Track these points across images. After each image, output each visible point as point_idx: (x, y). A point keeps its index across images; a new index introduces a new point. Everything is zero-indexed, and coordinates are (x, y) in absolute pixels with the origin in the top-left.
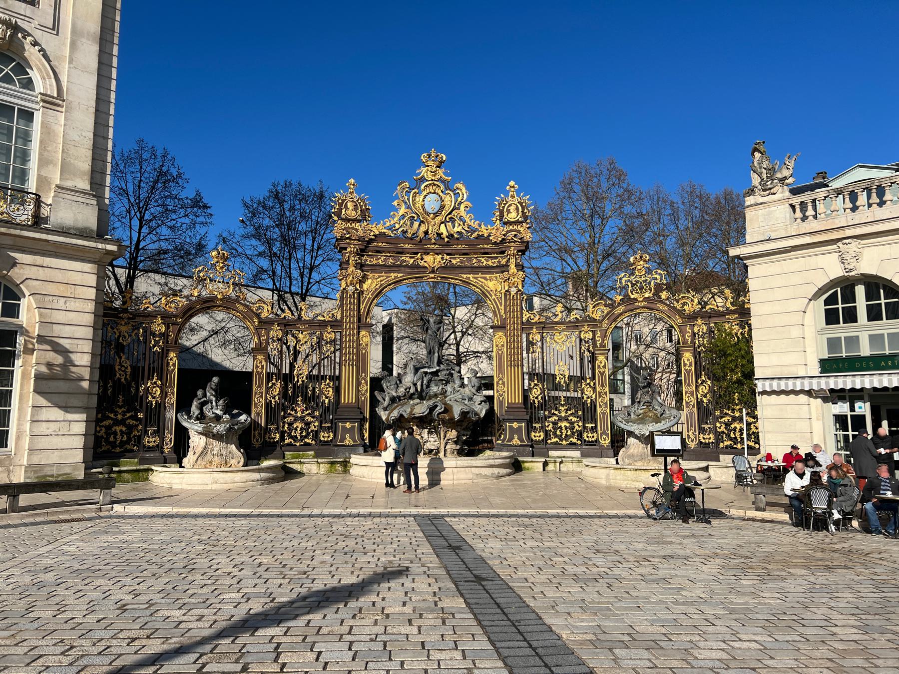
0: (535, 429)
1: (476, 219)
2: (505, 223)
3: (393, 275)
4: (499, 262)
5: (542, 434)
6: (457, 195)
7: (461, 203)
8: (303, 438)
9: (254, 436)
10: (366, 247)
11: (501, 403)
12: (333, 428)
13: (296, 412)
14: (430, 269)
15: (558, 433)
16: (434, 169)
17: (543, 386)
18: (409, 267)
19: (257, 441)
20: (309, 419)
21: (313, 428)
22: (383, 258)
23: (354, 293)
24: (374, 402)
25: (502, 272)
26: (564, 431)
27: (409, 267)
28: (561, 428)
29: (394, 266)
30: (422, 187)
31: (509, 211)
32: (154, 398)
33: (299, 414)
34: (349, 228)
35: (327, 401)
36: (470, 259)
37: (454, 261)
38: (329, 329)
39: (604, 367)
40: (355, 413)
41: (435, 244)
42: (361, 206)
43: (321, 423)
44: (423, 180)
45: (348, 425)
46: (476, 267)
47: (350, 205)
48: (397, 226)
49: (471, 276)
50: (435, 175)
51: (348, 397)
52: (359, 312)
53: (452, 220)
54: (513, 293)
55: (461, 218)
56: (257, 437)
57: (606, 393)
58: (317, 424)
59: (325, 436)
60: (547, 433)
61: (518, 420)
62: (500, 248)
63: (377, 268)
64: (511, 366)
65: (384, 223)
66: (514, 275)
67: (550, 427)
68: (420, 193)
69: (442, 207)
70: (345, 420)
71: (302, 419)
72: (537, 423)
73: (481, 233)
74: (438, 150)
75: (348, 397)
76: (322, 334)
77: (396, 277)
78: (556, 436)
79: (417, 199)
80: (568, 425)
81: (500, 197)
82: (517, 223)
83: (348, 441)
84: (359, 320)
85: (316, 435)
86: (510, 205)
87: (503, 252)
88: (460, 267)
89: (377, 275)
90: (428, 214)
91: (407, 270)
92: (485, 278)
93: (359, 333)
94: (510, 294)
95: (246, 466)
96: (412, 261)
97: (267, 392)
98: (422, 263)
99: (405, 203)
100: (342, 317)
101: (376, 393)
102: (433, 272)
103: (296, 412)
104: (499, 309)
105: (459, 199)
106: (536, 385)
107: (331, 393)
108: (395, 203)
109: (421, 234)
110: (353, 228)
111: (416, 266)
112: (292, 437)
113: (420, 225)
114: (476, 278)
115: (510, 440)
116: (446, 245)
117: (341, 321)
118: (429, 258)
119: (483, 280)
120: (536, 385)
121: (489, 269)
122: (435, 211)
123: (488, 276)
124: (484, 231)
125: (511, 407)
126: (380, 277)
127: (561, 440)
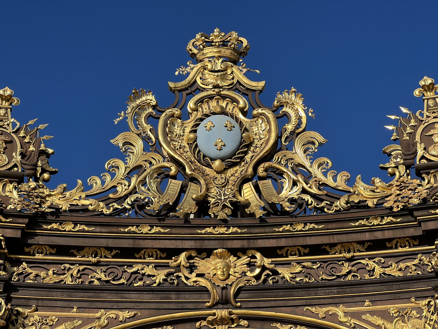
1: (337, 168)
2: (420, 173)
6: (283, 118)
7: (294, 134)
10: (26, 234)
14: (216, 294)
16: (219, 65)
18: (153, 291)
22: (75, 270)
27: (153, 291)
30: (191, 104)
37: (286, 273)
41: (225, 223)
44: (193, 88)
48: (121, 190)
49: (340, 311)
50: (223, 78)
53: (276, 175)
55: (298, 168)
65: (87, 187)
68: (184, 116)
69: (245, 145)
74: (226, 29)
79: (177, 130)
90: (206, 160)
91: (147, 297)
92: (385, 315)
96: (160, 275)
102: (224, 302)
105: (290, 127)
111: (174, 288)
116: (259, 230)
118: (212, 266)
122: (227, 151)
123: (392, 308)
124: (363, 191)
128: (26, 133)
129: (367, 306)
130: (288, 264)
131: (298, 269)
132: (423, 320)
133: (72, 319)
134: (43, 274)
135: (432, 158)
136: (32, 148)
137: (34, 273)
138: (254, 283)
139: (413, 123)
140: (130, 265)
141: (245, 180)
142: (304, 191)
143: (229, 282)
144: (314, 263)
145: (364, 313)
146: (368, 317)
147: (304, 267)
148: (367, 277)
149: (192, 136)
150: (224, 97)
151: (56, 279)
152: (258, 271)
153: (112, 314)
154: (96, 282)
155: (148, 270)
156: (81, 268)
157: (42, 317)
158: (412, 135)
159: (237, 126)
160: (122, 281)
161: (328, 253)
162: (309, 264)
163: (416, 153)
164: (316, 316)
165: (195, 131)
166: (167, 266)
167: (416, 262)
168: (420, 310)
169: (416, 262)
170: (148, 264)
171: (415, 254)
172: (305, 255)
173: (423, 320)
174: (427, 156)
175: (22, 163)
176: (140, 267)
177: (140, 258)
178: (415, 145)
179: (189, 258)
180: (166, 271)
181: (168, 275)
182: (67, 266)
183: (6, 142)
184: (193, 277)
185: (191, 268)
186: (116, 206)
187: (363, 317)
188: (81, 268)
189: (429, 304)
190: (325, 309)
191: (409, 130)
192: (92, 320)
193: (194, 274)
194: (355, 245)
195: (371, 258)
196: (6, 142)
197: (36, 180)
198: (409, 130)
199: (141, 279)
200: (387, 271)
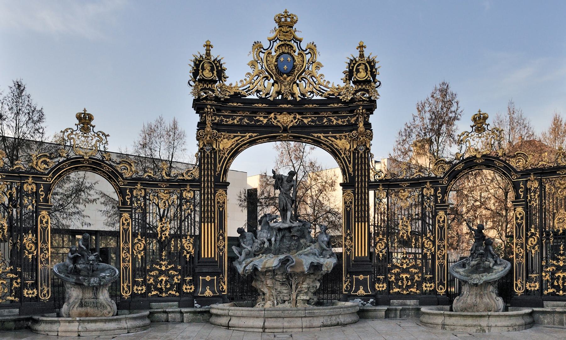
0: (379, 281)
3: (248, 135)
4: (348, 121)
5: (385, 285)
8: (167, 290)
9: (124, 289)
11: (348, 257)
12: (194, 282)
13: (161, 265)
15: (400, 284)
17: (387, 240)
19: (126, 293)
20: (173, 272)
21: (176, 281)
25: (351, 131)
26: (405, 282)
28: (402, 279)
29: (248, 125)
31: (358, 71)
32: (29, 253)
33: (163, 268)
34: (205, 89)
35: (188, 256)
36: (321, 119)
37: (306, 121)
39: (444, 221)
40: (213, 266)
42: (217, 67)
43: (183, 277)
45: (208, 278)
46: (326, 127)
49: (321, 135)
51: (208, 252)
52: (215, 171)
54: (361, 152)
56: (126, 289)
57: (444, 246)
58: (180, 277)
59: (187, 288)
60: (389, 284)
61: (364, 273)
63: (232, 129)
64: (358, 222)
67: (393, 279)
69: (294, 67)
70: (205, 274)
71: (165, 273)
72: (381, 275)
73: (331, 93)
75: (208, 252)
76: (181, 194)
77: (251, 137)
78: (399, 287)
80: (408, 276)
82: (367, 82)
83: (208, 293)
84: (217, 178)
85: (179, 287)
86: (360, 65)
87: (352, 111)
88: (310, 126)
89: (232, 135)
92: (335, 137)
93: (215, 193)
94: (358, 152)
95: (117, 315)
97: (133, 246)
98: (275, 122)
103: (161, 267)
104: (347, 167)
106: (380, 239)
110: (210, 89)
112: (156, 289)
113: (273, 85)
114: (326, 137)
115: (356, 291)
117: (199, 181)
119: (333, 139)
120: (380, 239)
121: (338, 129)
125: (357, 260)
126: (235, 137)
127: (403, 290)
129: (330, 134)
130: (306, 118)
131: (310, 120)
133: (238, 136)
134: (228, 120)
136: (220, 68)
140: (255, 117)
141: (294, 83)
144: (315, 117)
145: (329, 136)
146: (330, 138)
149: (276, 63)
150: (288, 45)
153: (250, 134)
155: (261, 119)
158: (353, 67)
164: (314, 137)
166: (267, 117)
168: (346, 136)
170: (261, 116)
179: (275, 114)
185: (275, 118)
189: (349, 135)
191: (352, 65)
195: (333, 117)
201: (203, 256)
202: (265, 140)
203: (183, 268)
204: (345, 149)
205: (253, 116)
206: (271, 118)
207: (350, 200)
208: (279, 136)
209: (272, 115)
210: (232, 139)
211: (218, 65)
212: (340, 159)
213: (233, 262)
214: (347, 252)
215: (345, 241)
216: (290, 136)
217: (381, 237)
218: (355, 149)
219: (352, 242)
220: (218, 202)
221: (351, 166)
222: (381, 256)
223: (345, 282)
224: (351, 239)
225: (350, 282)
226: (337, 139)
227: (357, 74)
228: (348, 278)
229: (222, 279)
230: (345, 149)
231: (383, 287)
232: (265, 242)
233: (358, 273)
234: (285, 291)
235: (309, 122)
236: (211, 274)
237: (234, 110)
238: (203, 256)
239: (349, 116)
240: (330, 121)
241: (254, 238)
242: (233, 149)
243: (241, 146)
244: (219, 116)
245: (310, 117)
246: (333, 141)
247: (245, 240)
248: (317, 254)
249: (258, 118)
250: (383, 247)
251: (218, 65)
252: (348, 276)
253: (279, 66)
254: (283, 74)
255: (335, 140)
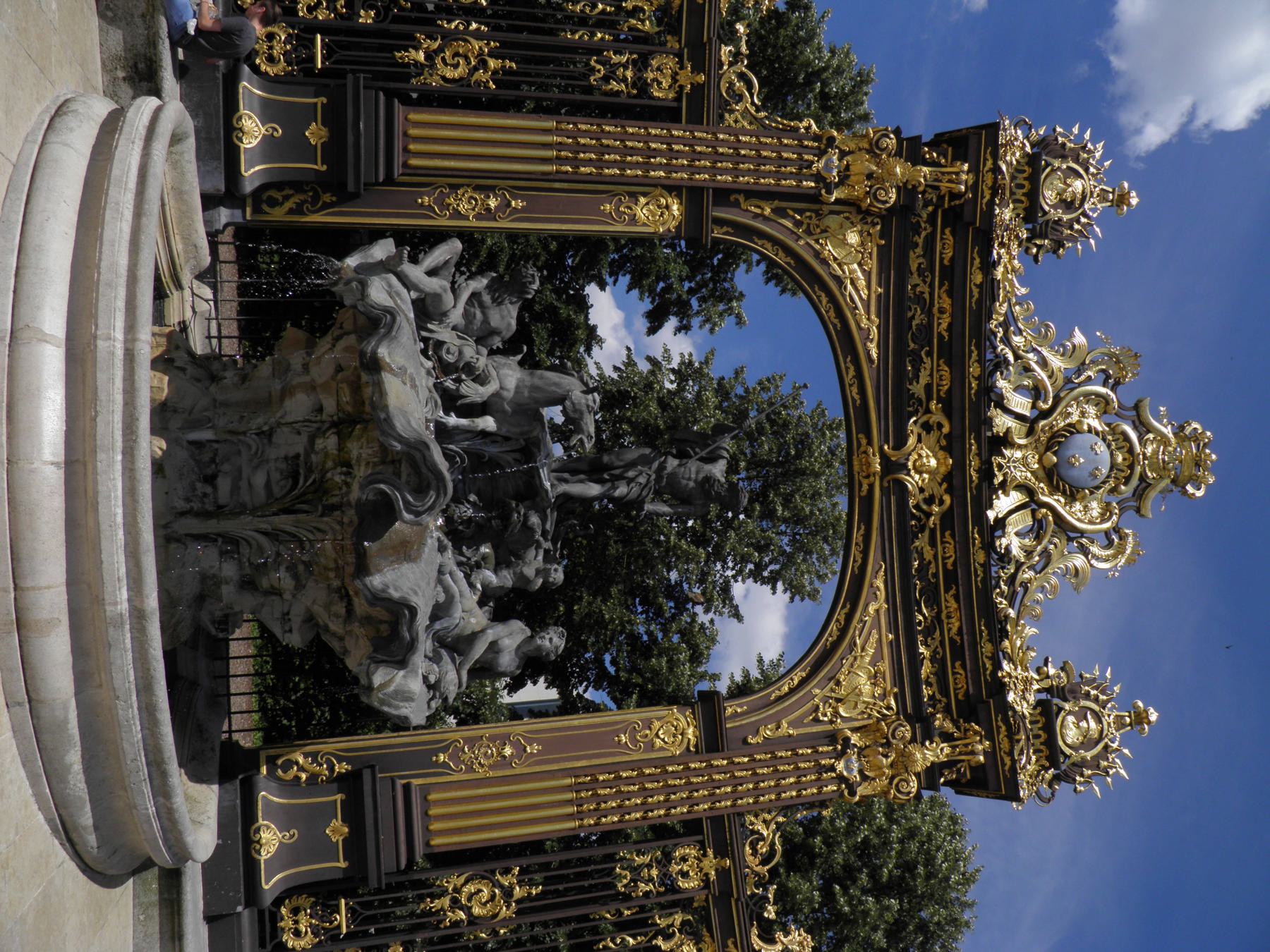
23: (818, 177)
24: (417, 242)
31: (1081, 715)
37: (922, 542)
38: (687, 78)
43: (324, 29)
47: (1078, 185)
48: (1017, 340)
54: (840, 766)
61: (355, 845)
62: (983, 703)
64: (577, 788)
66: (902, 764)
70: (334, 119)
75: (430, 135)
79: (1091, 410)
81: (1114, 681)
83: (253, 130)
84: (724, 195)
86: (1099, 719)
89: (872, 264)
96: (918, 389)
99: (1079, 372)
100: (729, 130)
101: (456, 245)
105: (1095, 549)
106: (508, 893)
107: (450, 73)
108: (1079, 338)
109: (1002, 422)
123: (885, 666)
126: (868, 275)
128: (1084, 225)
130: (933, 543)
131: (928, 555)
132: (871, 700)
134: (919, 251)
135: (1060, 719)
137: (920, 241)
138: (911, 502)
139: (1102, 697)
140: (929, 354)
142: (1019, 565)
143: (912, 472)
147: (930, 562)
148: (920, 638)
149: (1086, 427)
151: (914, 267)
152: (925, 507)
154: (910, 314)
156: (927, 296)
157: (870, 254)
158: (1087, 696)
159: (1097, 483)
160: (912, 345)
161: (946, 591)
162: (932, 570)
163: (1065, 700)
165: (1090, 431)
167: (938, 696)
168: (884, 696)
169: (938, 696)
170: (931, 375)
171: (947, 695)
172: (944, 565)
173: (871, 700)
174: (1063, 713)
175: (1048, 222)
176: (928, 366)
177: (938, 365)
178: (1076, 699)
180: (923, 397)
181: (920, 400)
182: (928, 280)
183: (1072, 202)
184: (916, 430)
186: (999, 335)
187: (874, 631)
188: (927, 296)
189: (889, 708)
190: (882, 586)
191: (1093, 692)
192: (868, 312)
193: (920, 430)
194: (957, 624)
195: (942, 643)
196: (1072, 202)
197: (1029, 240)
198: (1093, 692)
199: (913, 367)
200: (927, 663)
201: (413, 116)
202: (855, 390)
203: (365, 31)
204: (839, 700)
205: (930, 344)
206: (928, 411)
207: (658, 742)
208: (870, 443)
209: (937, 417)
210: (860, 265)
211: (1076, 226)
212: (803, 682)
213: (390, 241)
214: (444, 750)
215: (492, 739)
216: (871, 486)
217: (518, 892)
218: (847, 740)
219: (491, 767)
220: (634, 196)
221: (786, 729)
222: (437, 904)
223: (314, 756)
224: (504, 762)
225: (313, 778)
226: (873, 663)
227: (1070, 713)
228: (331, 768)
229: (314, 203)
230: (839, 700)
231: (297, 933)
232: (482, 385)
233: (353, 814)
234: (259, 480)
235: (921, 555)
236: (335, 149)
237: (953, 276)
238: (412, 116)
239: (948, 705)
240: (928, 632)
241: (497, 343)
242: (824, 262)
243: (833, 299)
244: (932, 219)
245: (935, 556)
246: (863, 649)
247: (487, 298)
248: (437, 626)
249: (927, 360)
250: (477, 911)
251: (1076, 226)
252: (341, 768)
253: (1078, 436)
254: (1055, 453)
255: (868, 659)
